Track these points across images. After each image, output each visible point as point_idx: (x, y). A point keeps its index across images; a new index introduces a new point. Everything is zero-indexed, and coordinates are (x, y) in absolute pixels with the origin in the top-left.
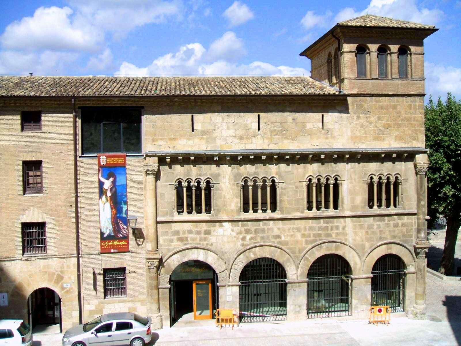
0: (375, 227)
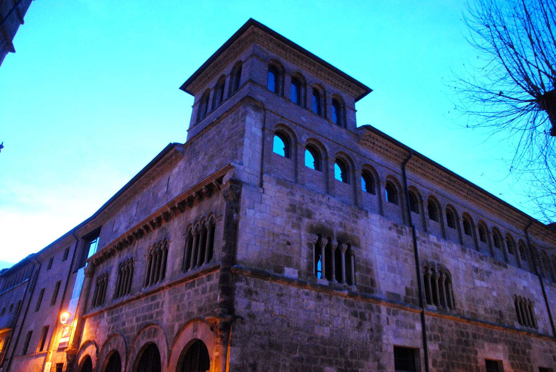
0: (186, 297)
